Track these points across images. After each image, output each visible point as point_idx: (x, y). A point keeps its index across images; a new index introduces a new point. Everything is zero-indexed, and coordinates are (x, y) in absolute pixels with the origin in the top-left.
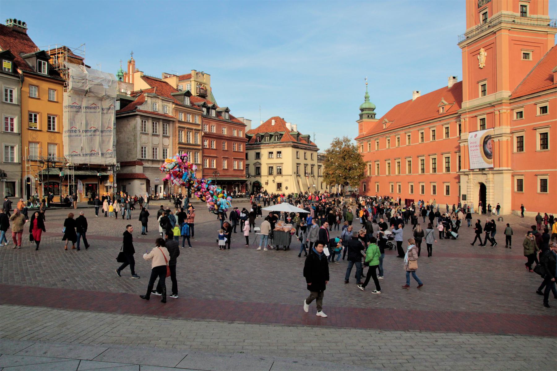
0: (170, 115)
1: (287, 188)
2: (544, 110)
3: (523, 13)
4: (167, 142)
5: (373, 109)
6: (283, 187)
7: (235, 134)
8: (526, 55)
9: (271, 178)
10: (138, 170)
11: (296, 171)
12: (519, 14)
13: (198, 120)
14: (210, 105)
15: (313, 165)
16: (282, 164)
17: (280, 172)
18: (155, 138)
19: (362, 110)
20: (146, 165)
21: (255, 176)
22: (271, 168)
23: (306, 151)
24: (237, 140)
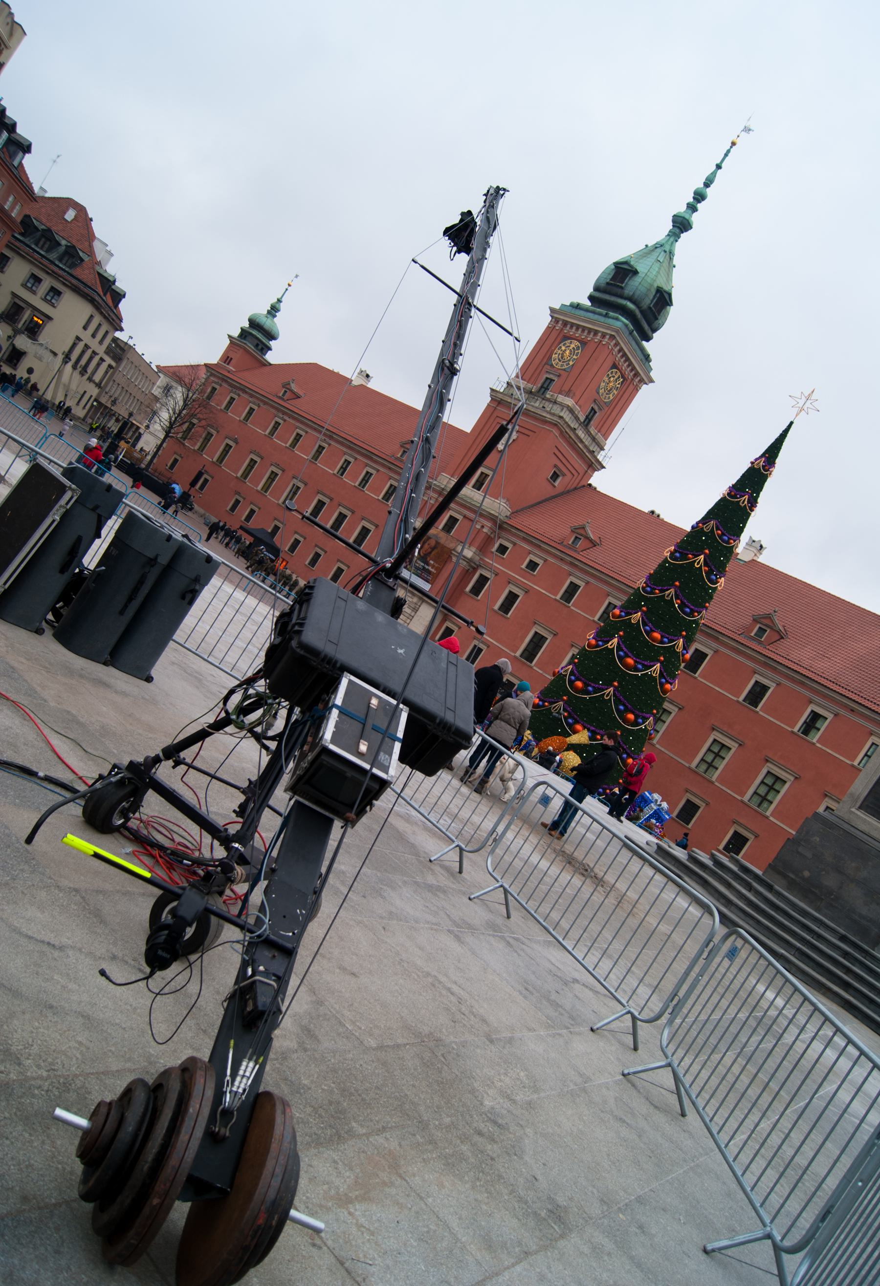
2: (533, 566)
5: (272, 337)
6: (25, 364)
8: (555, 476)
12: (582, 418)
15: (94, 353)
16: (50, 318)
17: (33, 331)
19: (253, 323)
23: (104, 321)
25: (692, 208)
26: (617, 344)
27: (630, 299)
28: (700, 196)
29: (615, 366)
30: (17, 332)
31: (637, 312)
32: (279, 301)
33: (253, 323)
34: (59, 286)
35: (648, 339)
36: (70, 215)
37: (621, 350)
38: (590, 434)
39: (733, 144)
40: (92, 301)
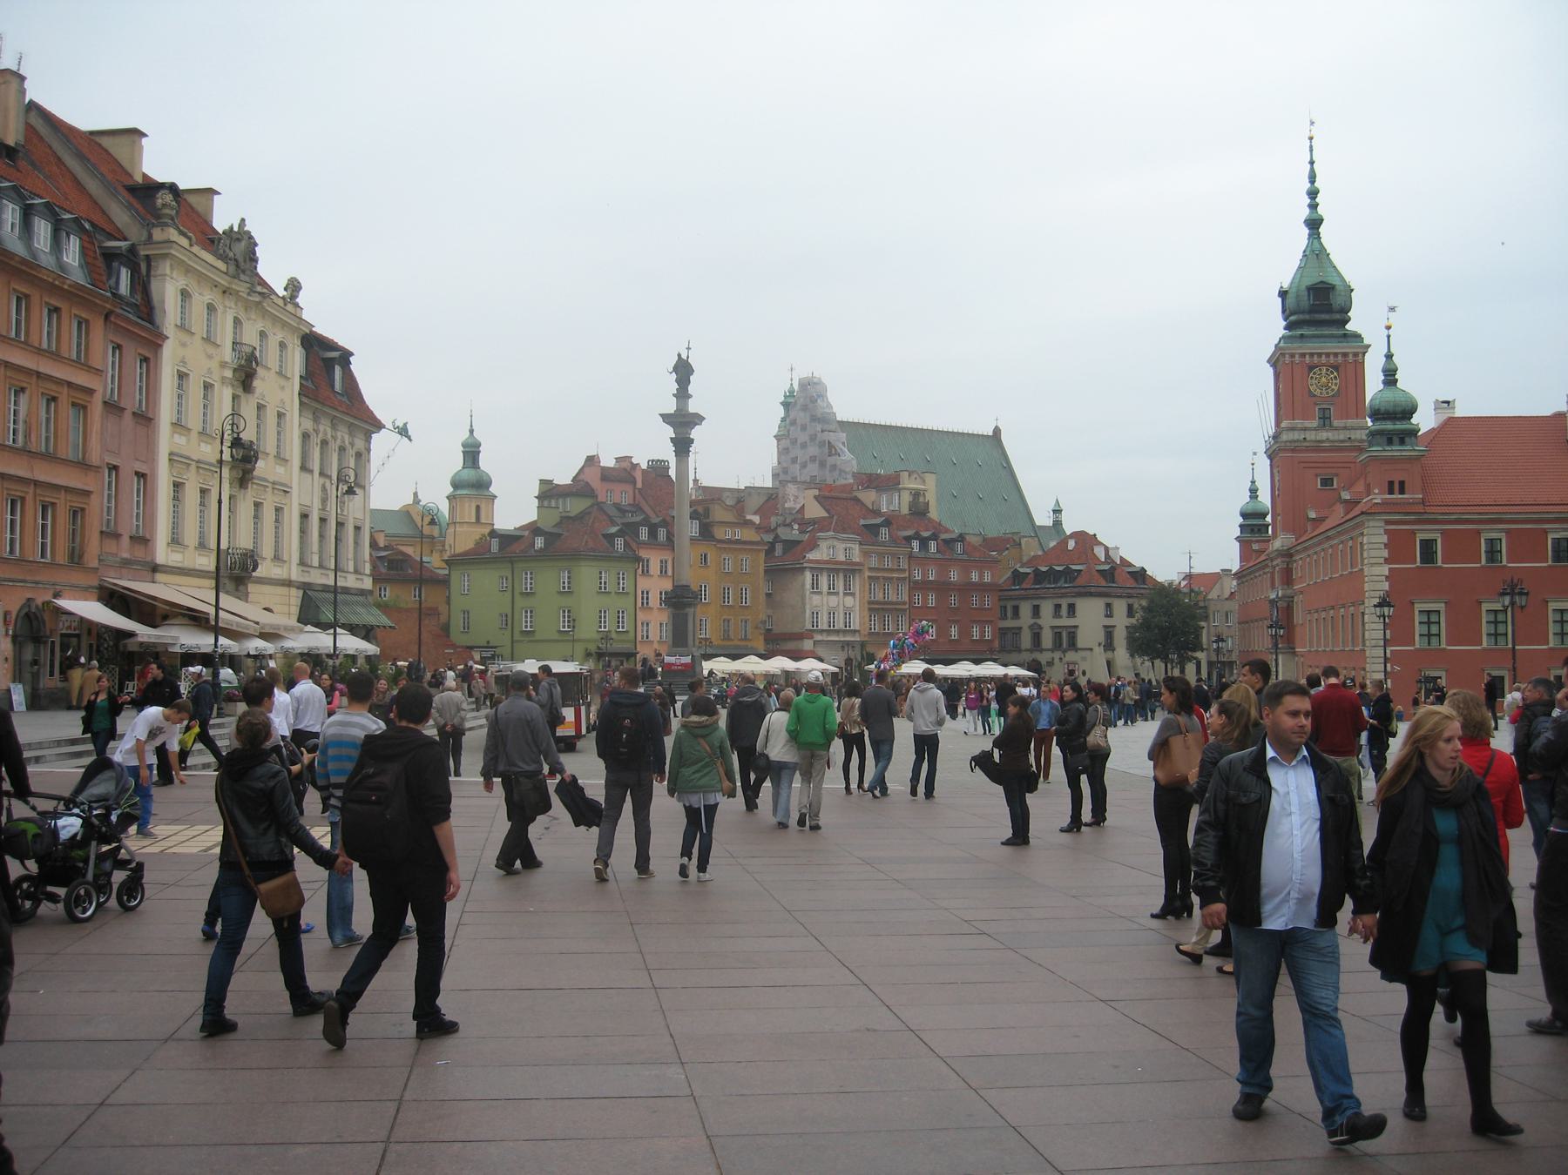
0: (856, 559)
1: (1084, 673)
3: (1325, 420)
4: (849, 601)
5: (1265, 515)
7: (975, 577)
8: (1327, 482)
9: (1057, 655)
10: (808, 645)
11: (1101, 637)
12: (1315, 423)
13: (904, 564)
14: (926, 534)
17: (1072, 645)
18: (833, 599)
20: (818, 637)
21: (1031, 651)
22: (1057, 636)
23: (1131, 601)
24: (982, 588)
25: (1313, 206)
26: (1292, 356)
27: (1292, 314)
28: (1313, 194)
29: (1311, 368)
30: (1064, 652)
31: (1301, 317)
32: (1253, 482)
33: (1244, 515)
34: (1071, 601)
35: (1347, 321)
36: (1071, 544)
37: (1303, 355)
38: (1337, 429)
39: (1311, 138)
40: (1091, 595)
